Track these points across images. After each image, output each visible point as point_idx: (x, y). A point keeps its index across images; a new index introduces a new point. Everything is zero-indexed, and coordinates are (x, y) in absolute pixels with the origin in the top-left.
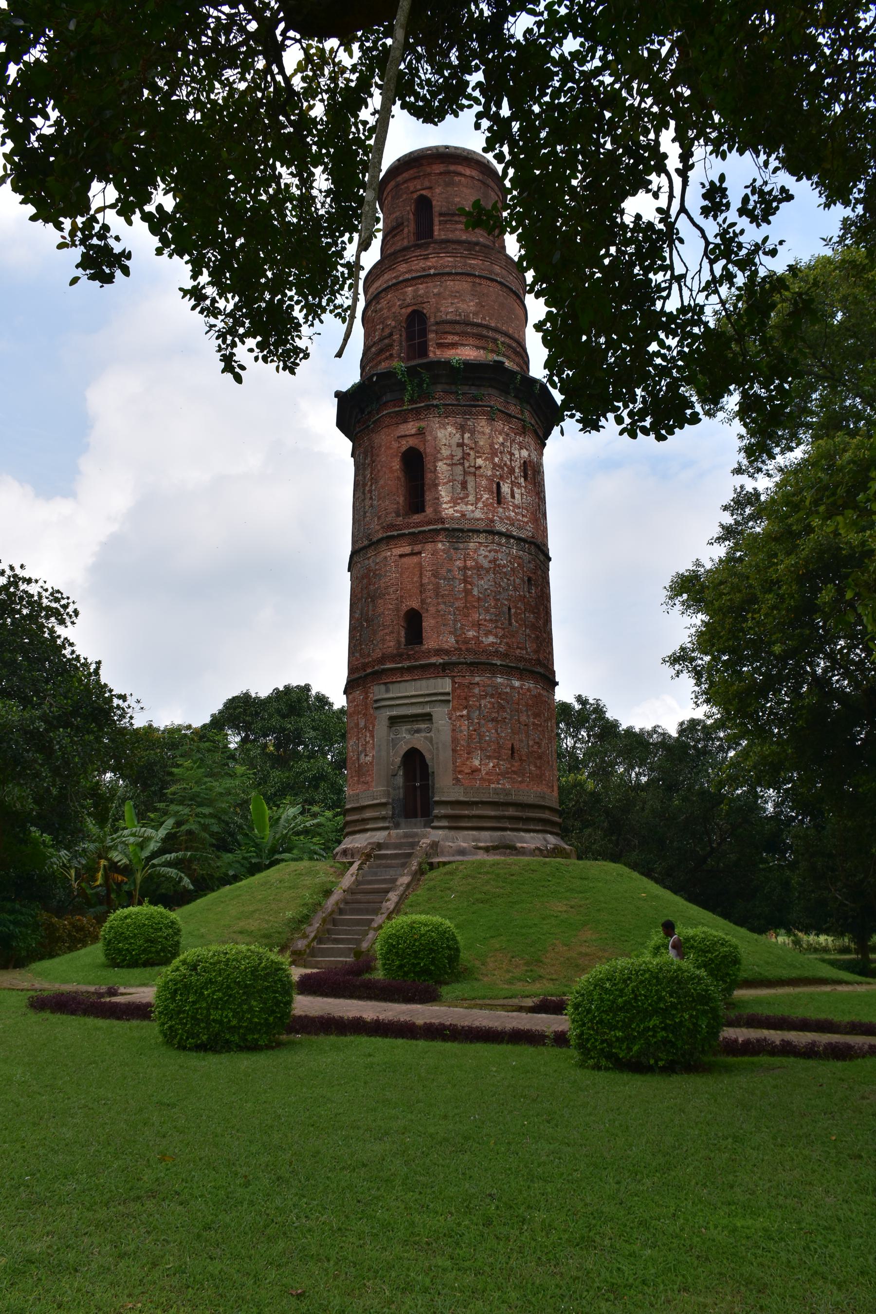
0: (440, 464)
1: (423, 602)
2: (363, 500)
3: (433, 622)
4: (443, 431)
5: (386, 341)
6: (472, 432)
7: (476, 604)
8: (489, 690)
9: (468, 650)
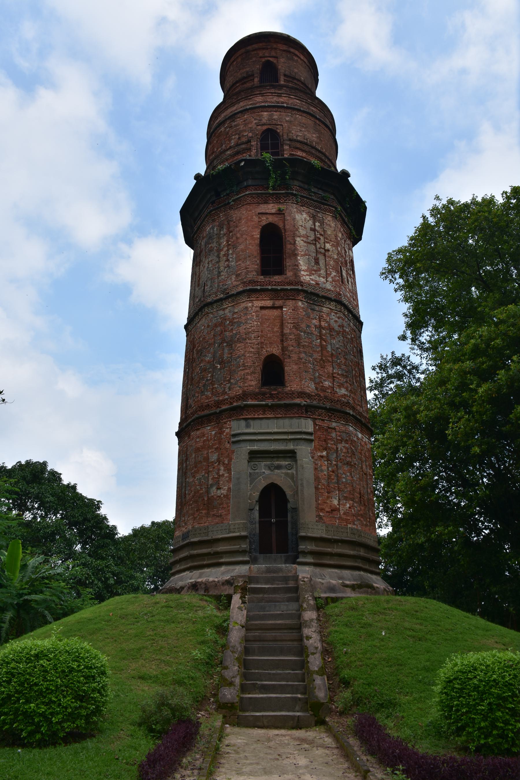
0: (298, 239)
1: (284, 349)
2: (218, 262)
3: (295, 367)
4: (299, 215)
5: (243, 146)
6: (322, 223)
7: (330, 359)
8: (344, 435)
9: (326, 397)
